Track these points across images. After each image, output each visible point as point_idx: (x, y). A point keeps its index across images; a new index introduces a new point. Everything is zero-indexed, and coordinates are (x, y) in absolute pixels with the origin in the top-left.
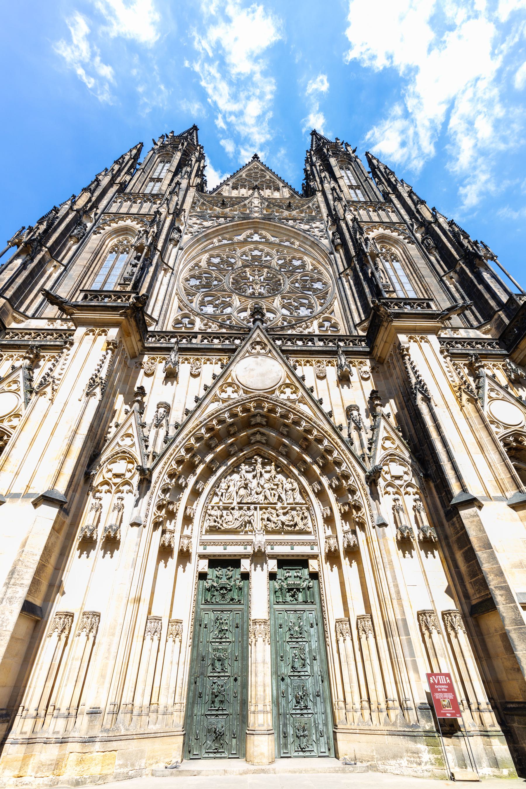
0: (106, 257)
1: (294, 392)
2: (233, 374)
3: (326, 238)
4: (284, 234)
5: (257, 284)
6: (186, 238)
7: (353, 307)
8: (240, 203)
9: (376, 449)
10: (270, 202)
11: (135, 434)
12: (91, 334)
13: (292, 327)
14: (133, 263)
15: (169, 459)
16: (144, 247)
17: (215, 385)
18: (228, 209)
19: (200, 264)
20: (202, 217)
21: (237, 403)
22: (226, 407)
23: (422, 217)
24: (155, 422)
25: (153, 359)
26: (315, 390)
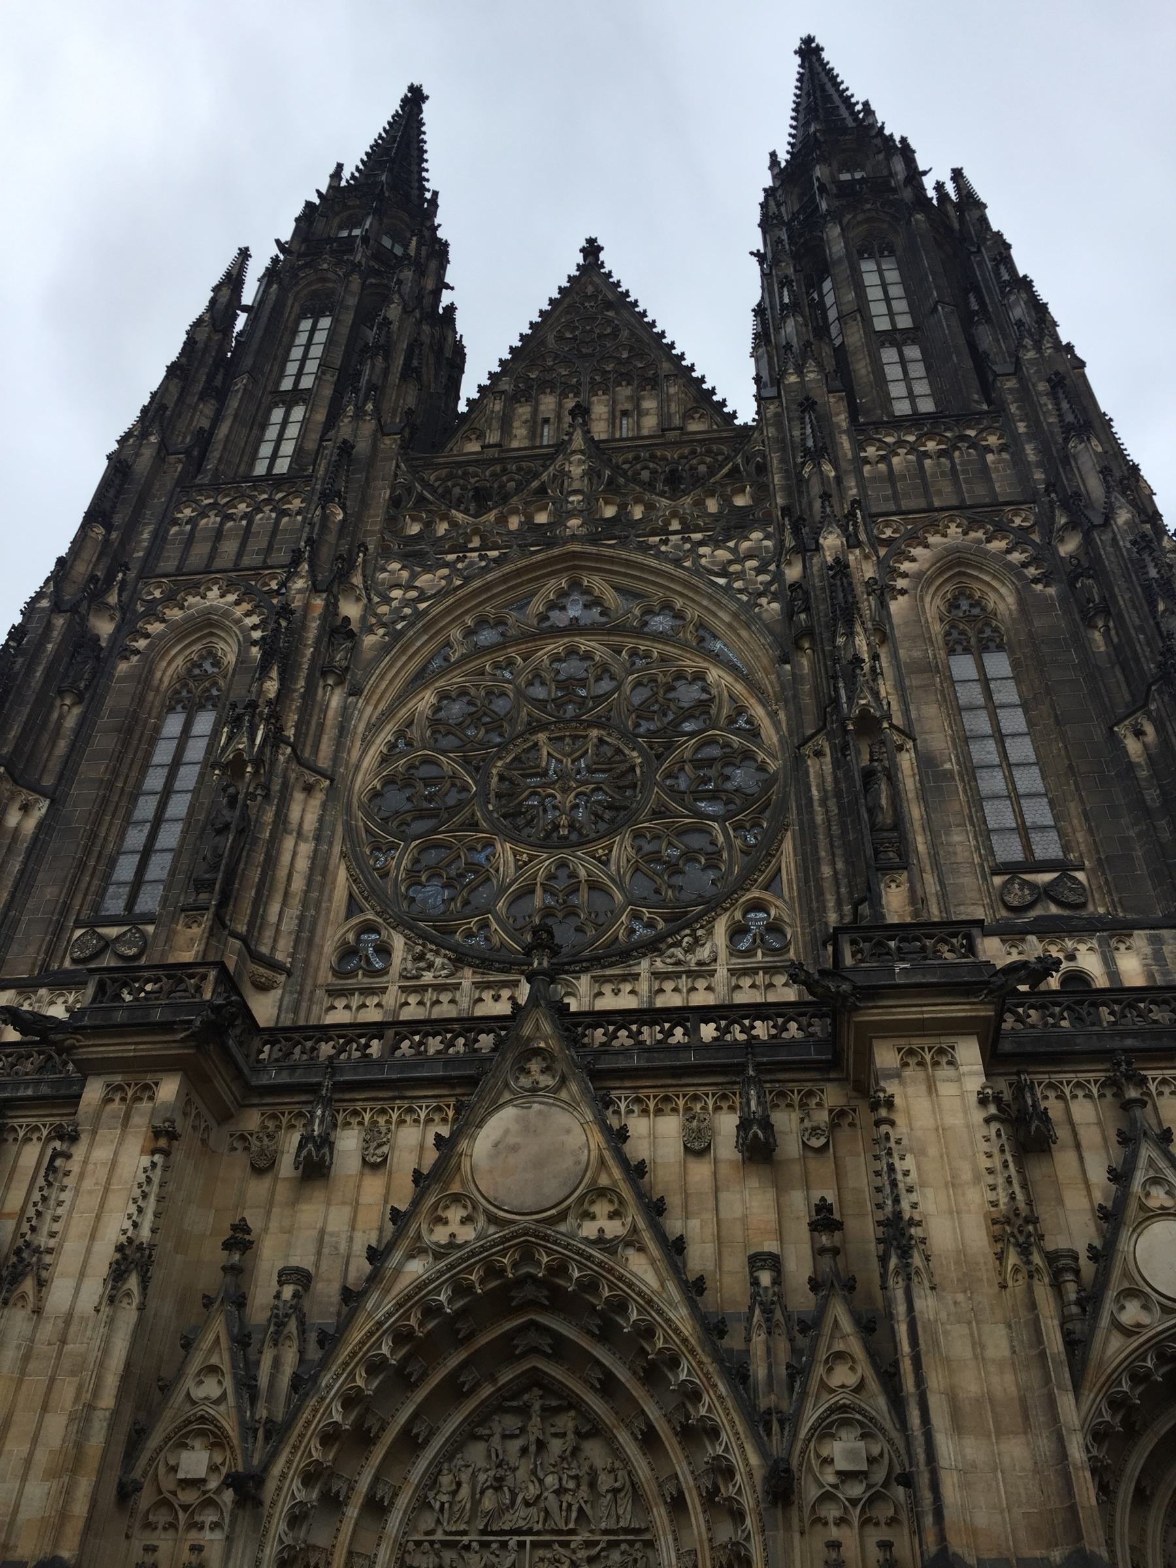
0: (157, 729)
1: (612, 1216)
2: (466, 1165)
3: (775, 597)
5: (565, 791)
6: (369, 640)
7: (826, 871)
8: (529, 483)
9: (804, 1395)
10: (616, 468)
11: (226, 1367)
12: (117, 1099)
13: (653, 947)
15: (302, 1436)
16: (244, 764)
17: (416, 1203)
18: (492, 516)
21: (469, 1258)
22: (441, 1273)
23: (1077, 495)
24: (272, 1329)
25: (274, 1117)
26: (674, 1201)
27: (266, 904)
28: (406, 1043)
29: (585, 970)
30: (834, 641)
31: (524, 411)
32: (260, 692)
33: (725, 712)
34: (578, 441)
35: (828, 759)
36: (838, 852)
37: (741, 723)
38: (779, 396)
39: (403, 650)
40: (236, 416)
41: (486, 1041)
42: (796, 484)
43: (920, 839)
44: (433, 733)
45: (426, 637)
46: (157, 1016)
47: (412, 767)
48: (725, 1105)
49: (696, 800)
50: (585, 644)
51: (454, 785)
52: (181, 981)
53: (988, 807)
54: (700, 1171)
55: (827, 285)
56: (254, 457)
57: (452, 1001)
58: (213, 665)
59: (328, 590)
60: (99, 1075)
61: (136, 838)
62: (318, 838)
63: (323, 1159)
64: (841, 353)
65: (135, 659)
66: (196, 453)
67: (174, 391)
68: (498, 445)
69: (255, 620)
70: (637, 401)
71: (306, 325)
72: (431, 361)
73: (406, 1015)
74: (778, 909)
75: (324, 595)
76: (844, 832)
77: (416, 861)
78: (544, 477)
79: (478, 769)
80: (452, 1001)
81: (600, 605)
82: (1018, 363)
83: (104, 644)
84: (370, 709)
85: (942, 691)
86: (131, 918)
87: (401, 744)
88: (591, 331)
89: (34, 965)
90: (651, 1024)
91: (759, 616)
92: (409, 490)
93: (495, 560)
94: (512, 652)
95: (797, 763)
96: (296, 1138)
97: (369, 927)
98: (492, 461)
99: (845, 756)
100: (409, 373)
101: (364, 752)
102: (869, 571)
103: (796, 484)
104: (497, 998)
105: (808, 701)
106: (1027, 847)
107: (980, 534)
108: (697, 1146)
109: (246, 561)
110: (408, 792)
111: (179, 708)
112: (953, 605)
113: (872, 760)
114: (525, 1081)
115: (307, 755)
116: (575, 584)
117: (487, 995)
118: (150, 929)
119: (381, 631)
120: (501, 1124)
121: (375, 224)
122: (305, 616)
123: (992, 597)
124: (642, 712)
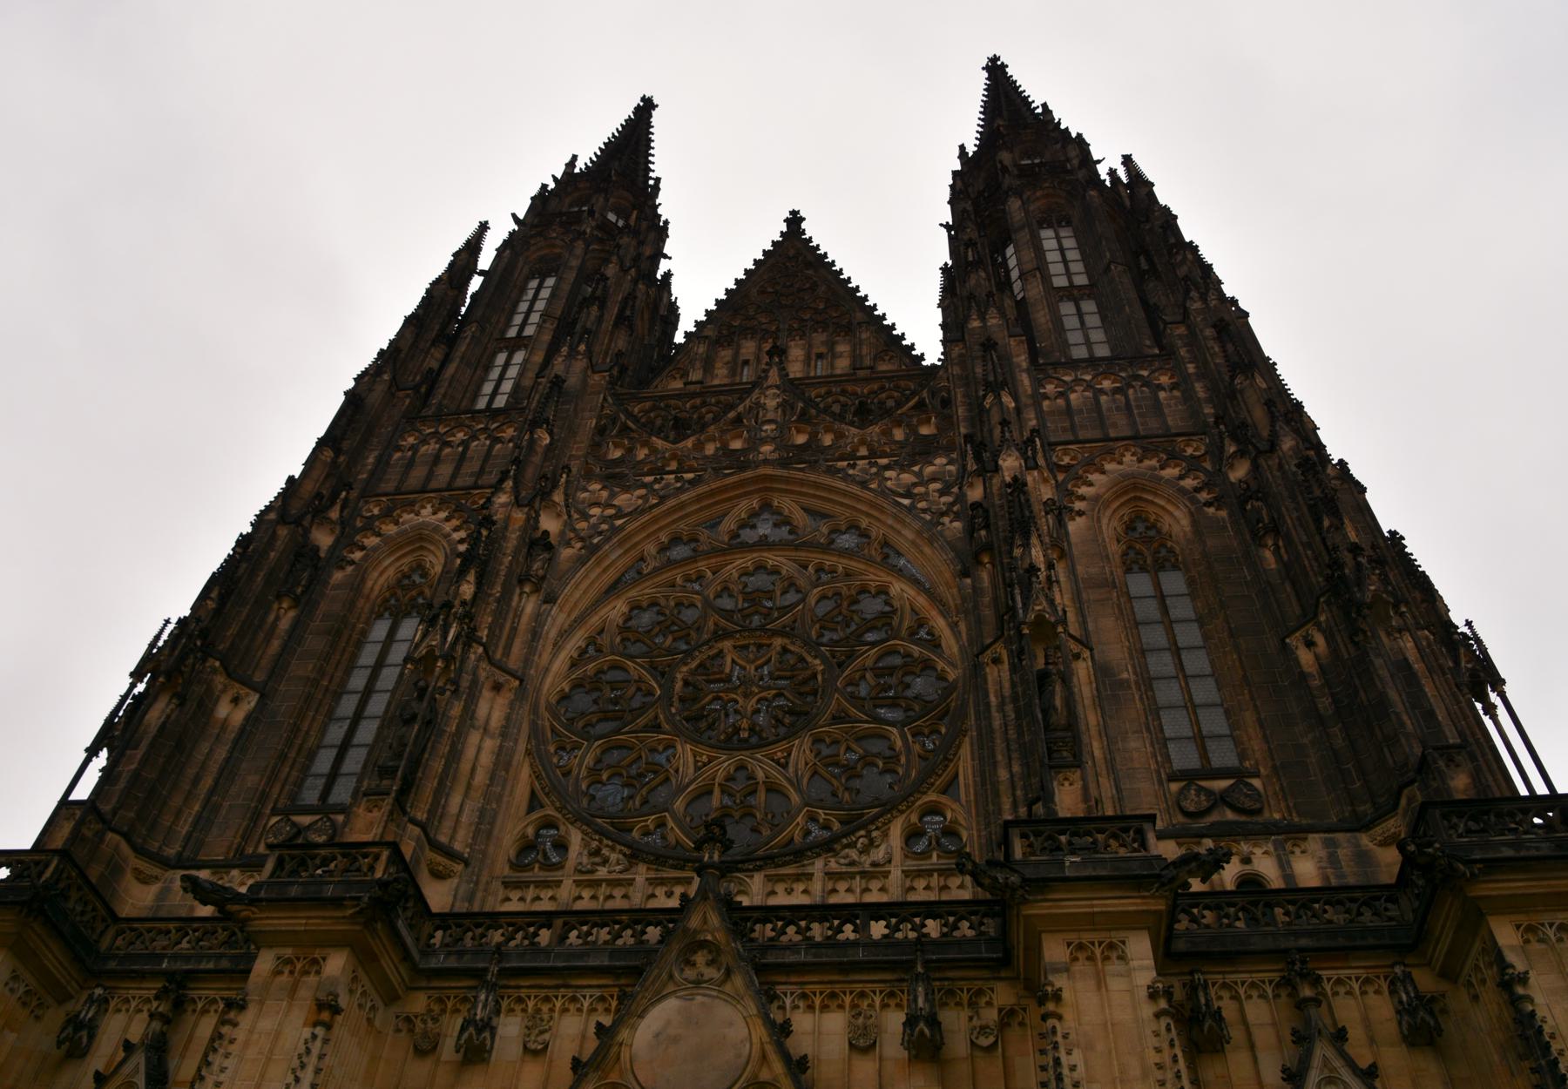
0: (364, 633)
2: (625, 1055)
3: (957, 517)
4: (842, 504)
5: (746, 696)
6: (566, 553)
7: (1003, 774)
8: (725, 413)
10: (809, 402)
12: (286, 972)
13: (827, 847)
16: (436, 659)
18: (689, 443)
19: (599, 641)
20: (615, 478)
25: (440, 1000)
27: (448, 795)
28: (574, 933)
29: (759, 869)
30: (1011, 552)
31: (726, 354)
32: (457, 593)
33: (906, 624)
34: (774, 377)
35: (1006, 666)
36: (1015, 755)
37: (923, 633)
38: (963, 340)
39: (598, 563)
40: (462, 358)
41: (653, 933)
42: (979, 414)
43: (1096, 745)
44: (623, 640)
46: (329, 891)
47: (600, 671)
48: (892, 1002)
49: (875, 706)
50: (772, 559)
51: (639, 689)
52: (355, 859)
53: (1166, 717)
54: (865, 1068)
55: (1010, 251)
56: (476, 394)
57: (625, 896)
58: (421, 576)
59: (530, 504)
61: (336, 733)
62: (504, 733)
63: (483, 1043)
64: (1022, 305)
65: (350, 569)
66: (423, 390)
68: (700, 382)
69: (462, 534)
70: (831, 345)
71: (534, 284)
72: (646, 316)
73: (579, 906)
74: (956, 812)
76: (1020, 734)
77: (598, 761)
78: (740, 408)
79: (664, 674)
80: (625, 896)
81: (788, 523)
82: (1186, 313)
83: (322, 555)
84: (562, 617)
85: (1119, 606)
86: (324, 808)
87: (591, 650)
89: (230, 847)
90: (821, 920)
91: (941, 533)
92: (614, 420)
93: (690, 482)
94: (702, 565)
95: (976, 671)
96: (460, 1021)
97: (550, 824)
98: (693, 395)
99: (1021, 660)
100: (621, 320)
101: (554, 655)
102: (1047, 493)
103: (979, 414)
104: (669, 895)
105: (988, 613)
106: (1204, 754)
107: (1154, 462)
108: (862, 1044)
109: (459, 482)
110: (595, 695)
111: (387, 615)
112: (1130, 527)
113: (1047, 663)
114: (690, 973)
115: (498, 656)
116: (766, 506)
117: (660, 891)
118: (340, 818)
119: (579, 545)
120: (662, 1015)
121: (607, 204)
122: (506, 528)
123: (1167, 519)
124: (826, 623)
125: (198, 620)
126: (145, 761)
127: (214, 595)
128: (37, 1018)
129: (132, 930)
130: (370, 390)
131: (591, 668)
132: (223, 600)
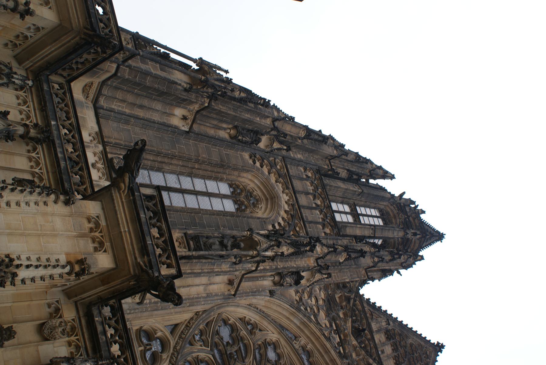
0: (221, 180)
8: (371, 356)
12: (92, 225)
14: (225, 241)
16: (256, 250)
18: (355, 342)
25: (73, 328)
40: (347, 189)
44: (259, 345)
45: (298, 324)
47: (242, 339)
58: (253, 203)
60: (103, 209)
66: (330, 172)
67: (351, 157)
69: (282, 223)
75: (316, 265)
84: (262, 303)
87: (249, 327)
88: (418, 361)
89: (109, 137)
92: (350, 291)
93: (340, 352)
97: (164, 344)
125: (232, 90)
126: (156, 77)
127: (243, 95)
128: (6, 45)
129: (64, 93)
130: (329, 145)
131: (244, 333)
132: (240, 100)
